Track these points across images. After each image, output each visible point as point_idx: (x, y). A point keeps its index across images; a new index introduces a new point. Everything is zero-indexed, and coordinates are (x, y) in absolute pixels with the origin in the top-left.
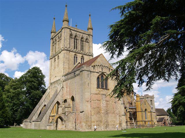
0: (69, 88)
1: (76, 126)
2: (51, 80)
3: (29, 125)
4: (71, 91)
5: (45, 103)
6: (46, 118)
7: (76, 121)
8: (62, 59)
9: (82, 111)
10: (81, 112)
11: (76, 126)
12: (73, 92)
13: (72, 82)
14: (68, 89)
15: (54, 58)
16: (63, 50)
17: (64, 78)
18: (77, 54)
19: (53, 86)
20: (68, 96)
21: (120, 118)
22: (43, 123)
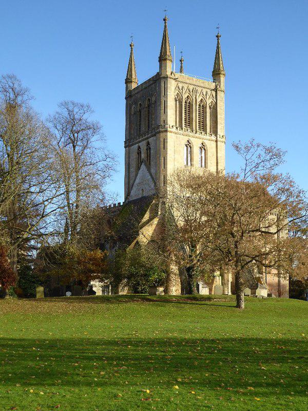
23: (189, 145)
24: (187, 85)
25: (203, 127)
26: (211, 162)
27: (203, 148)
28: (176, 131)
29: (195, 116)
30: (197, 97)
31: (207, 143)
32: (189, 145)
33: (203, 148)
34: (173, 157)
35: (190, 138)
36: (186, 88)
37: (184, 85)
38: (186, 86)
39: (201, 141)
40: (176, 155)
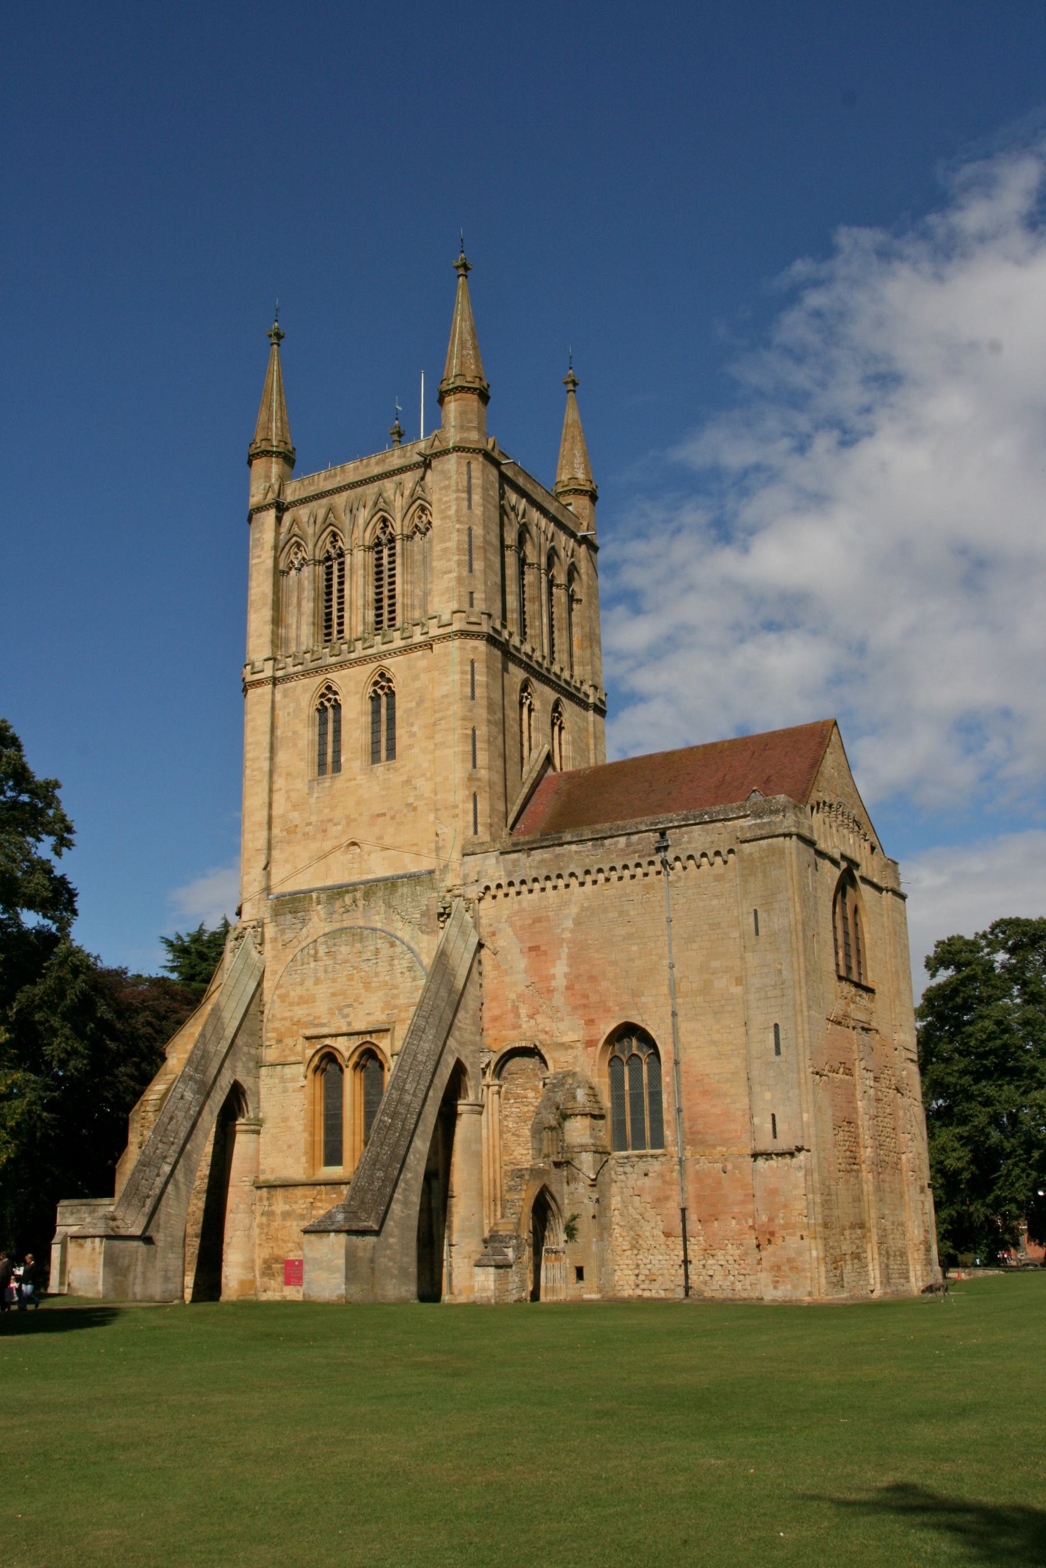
0: (574, 960)
1: (686, 1262)
2: (278, 873)
3: (139, 1268)
4: (604, 984)
5: (234, 1072)
6: (406, 1203)
7: (693, 1225)
8: (456, 709)
9: (784, 1143)
10: (768, 1155)
11: (686, 1262)
12: (636, 994)
13: (613, 914)
14: (560, 969)
15: (319, 679)
16: (464, 634)
17: (493, 868)
18: (535, 683)
19: (318, 922)
20: (563, 1026)
21: (923, 1203)
22: (390, 1246)
23: (328, 708)
24: (324, 501)
25: (383, 612)
26: (415, 729)
27: (383, 695)
28: (279, 674)
29: (358, 590)
30: (361, 521)
31: (394, 665)
32: (328, 708)
33: (383, 695)
34: (266, 765)
35: (329, 676)
36: (321, 513)
37: (314, 504)
38: (320, 508)
39: (365, 673)
40: (281, 757)
